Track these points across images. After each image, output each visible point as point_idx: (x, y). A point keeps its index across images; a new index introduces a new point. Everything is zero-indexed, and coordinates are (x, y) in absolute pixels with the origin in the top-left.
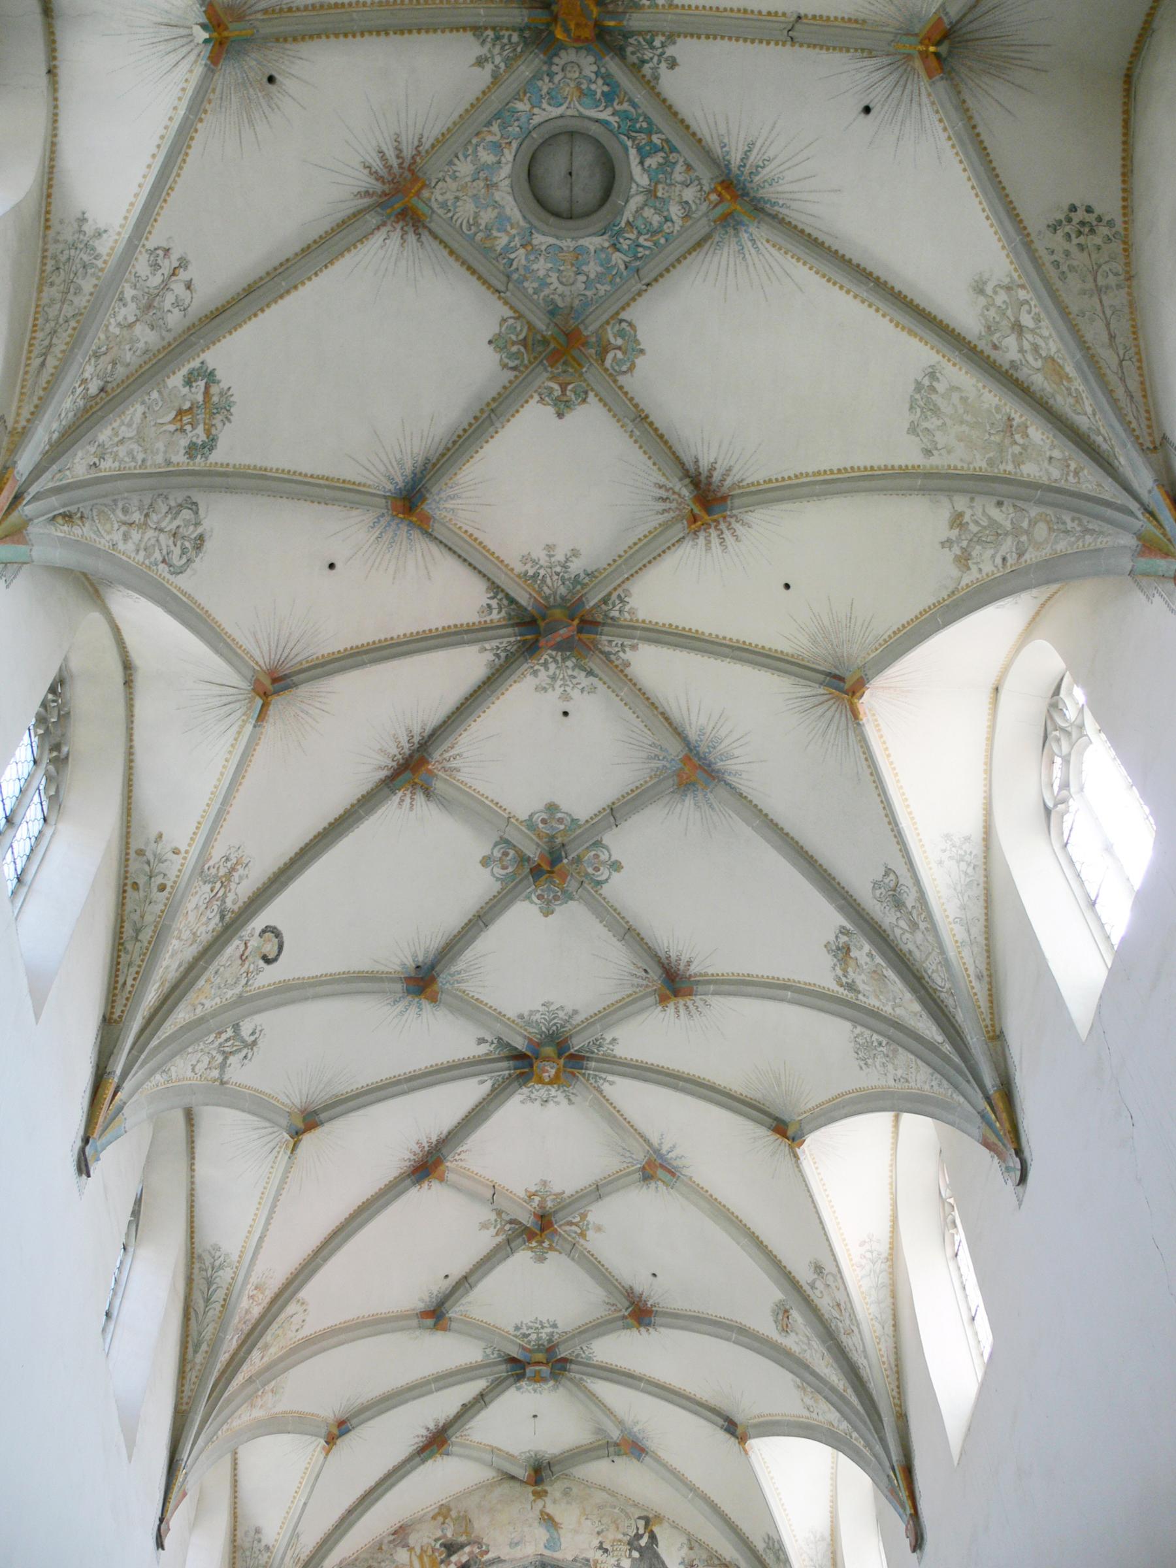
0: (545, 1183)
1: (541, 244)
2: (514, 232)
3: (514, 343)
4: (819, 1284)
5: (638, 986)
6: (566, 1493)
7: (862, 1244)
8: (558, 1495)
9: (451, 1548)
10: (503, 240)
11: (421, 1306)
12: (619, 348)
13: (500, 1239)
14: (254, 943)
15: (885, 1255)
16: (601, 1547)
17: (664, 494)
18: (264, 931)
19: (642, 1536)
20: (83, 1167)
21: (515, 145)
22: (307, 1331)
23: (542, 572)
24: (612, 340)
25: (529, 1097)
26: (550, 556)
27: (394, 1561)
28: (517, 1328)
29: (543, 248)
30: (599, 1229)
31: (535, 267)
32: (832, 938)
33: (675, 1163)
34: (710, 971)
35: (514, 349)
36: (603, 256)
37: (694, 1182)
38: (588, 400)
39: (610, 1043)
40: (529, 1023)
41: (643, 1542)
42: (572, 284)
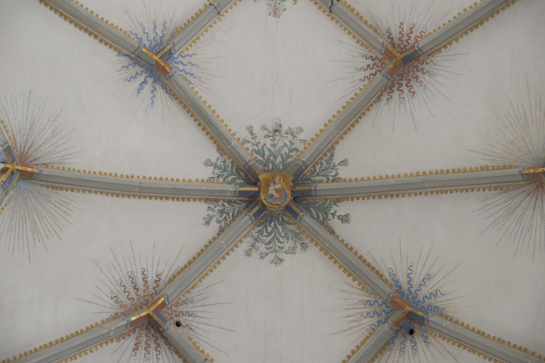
5: (185, 302)
25: (294, 137)
33: (138, 69)
37: (115, 49)
39: (211, 217)
40: (296, 235)
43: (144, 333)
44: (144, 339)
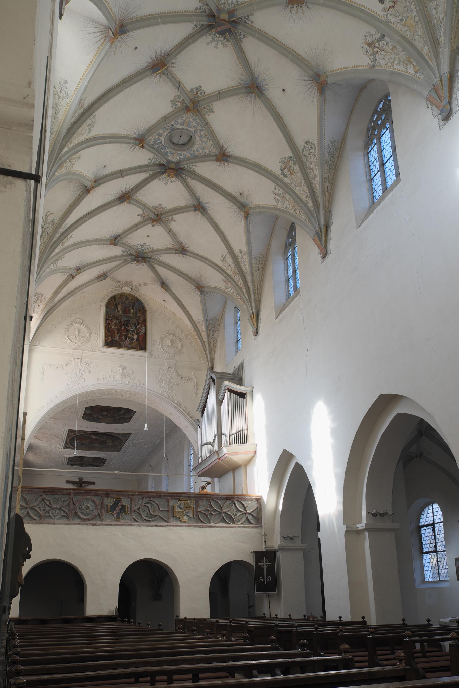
1: (193, 129)
2: (199, 134)
3: (208, 109)
10: (202, 133)
12: (177, 102)
17: (173, 65)
21: (193, 150)
23: (222, 39)
24: (179, 104)
26: (217, 44)
29: (192, 128)
31: (196, 124)
35: (208, 107)
36: (176, 123)
38: (190, 89)
42: (186, 118)
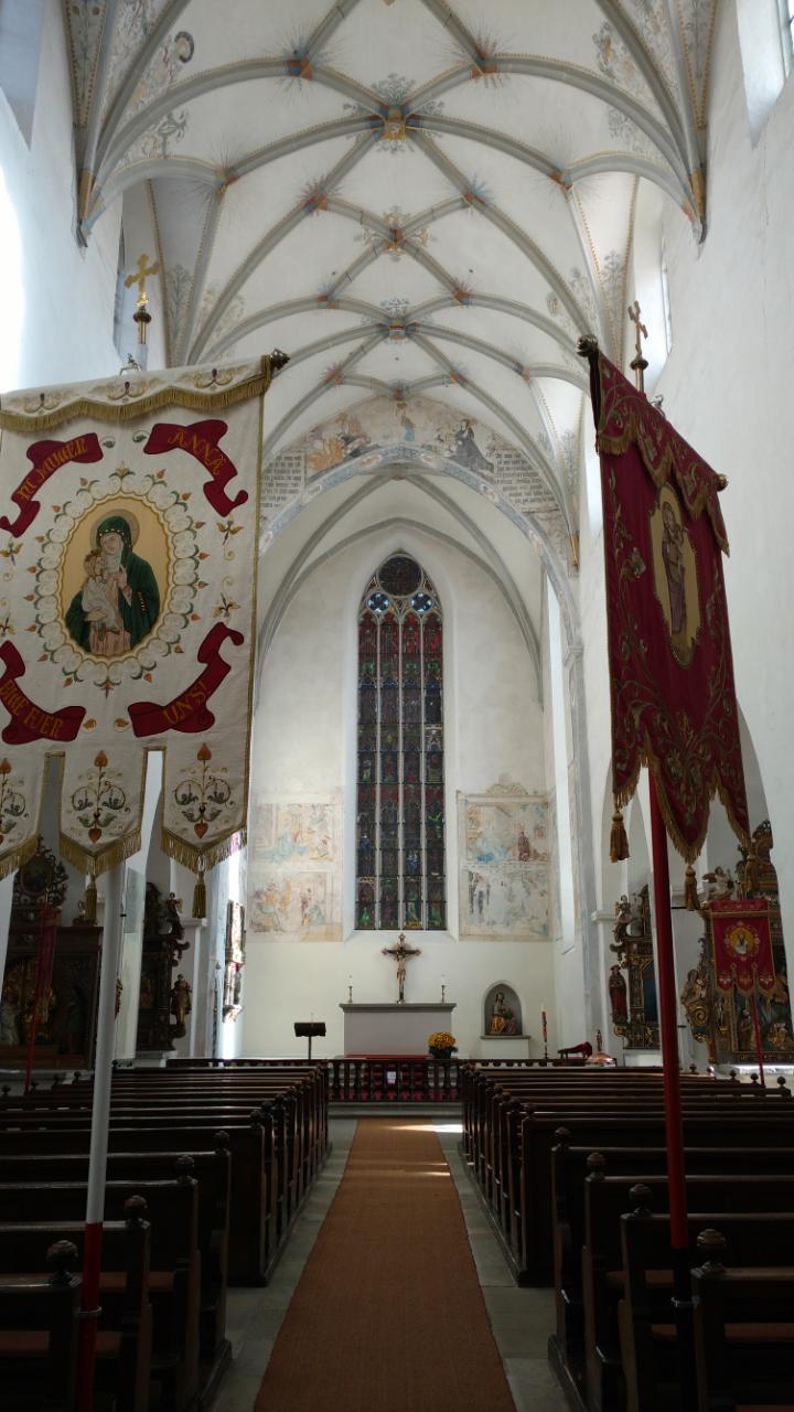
0: (396, 208)
4: (576, 284)
5: (459, 62)
6: (418, 405)
7: (607, 258)
8: (413, 407)
9: (348, 440)
11: (318, 293)
13: (369, 246)
14: (171, 48)
15: (621, 266)
16: (439, 439)
18: (178, 37)
19: (463, 432)
20: (82, 240)
22: (246, 315)
27: (313, 448)
28: (383, 304)
30: (434, 239)
32: (597, 31)
34: (510, 52)
41: (465, 435)
43: (489, 52)
44: (489, 48)
